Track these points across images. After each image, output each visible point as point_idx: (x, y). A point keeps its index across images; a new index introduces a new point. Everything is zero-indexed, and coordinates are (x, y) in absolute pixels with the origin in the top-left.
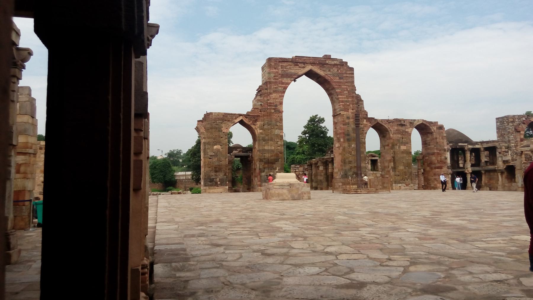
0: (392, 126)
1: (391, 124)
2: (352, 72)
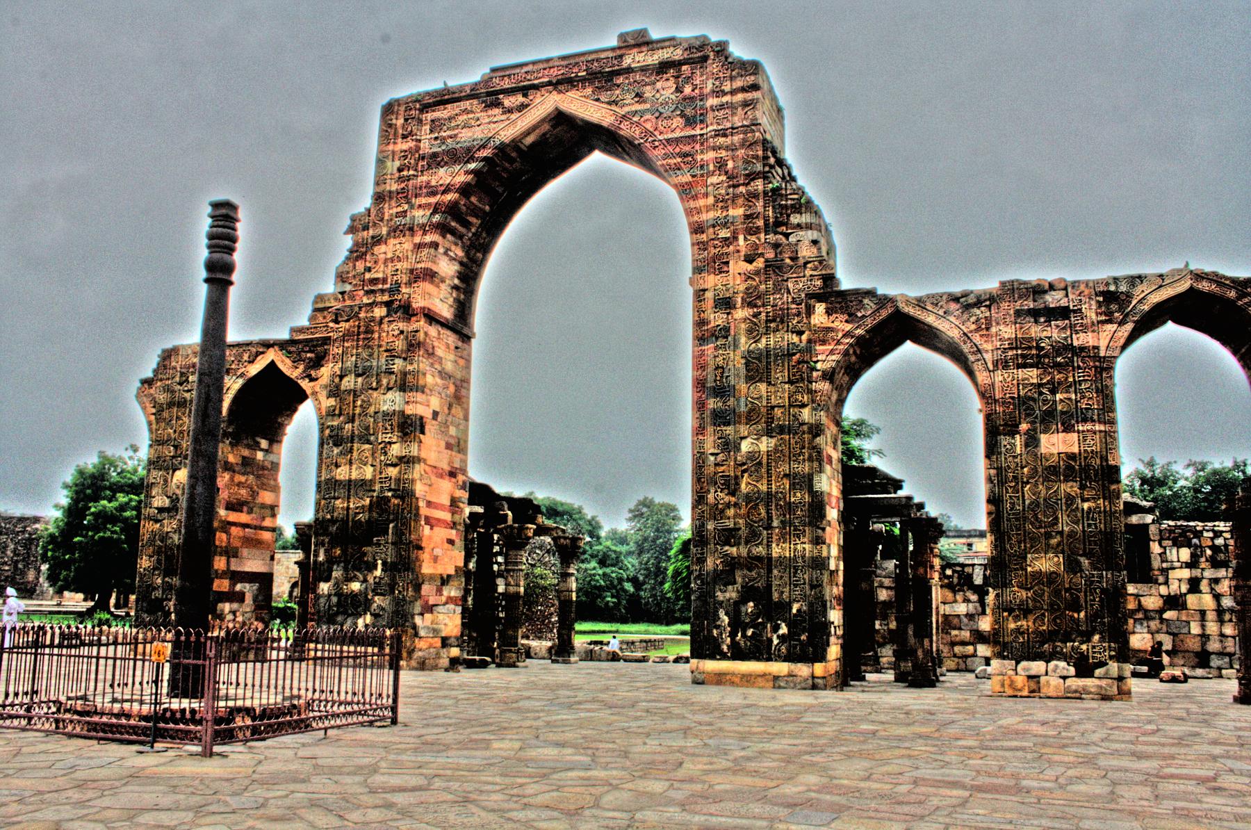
0: (985, 327)
1: (980, 312)
2: (750, 80)
